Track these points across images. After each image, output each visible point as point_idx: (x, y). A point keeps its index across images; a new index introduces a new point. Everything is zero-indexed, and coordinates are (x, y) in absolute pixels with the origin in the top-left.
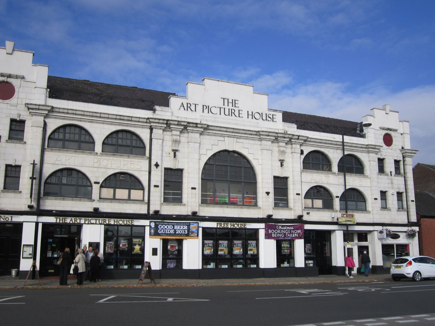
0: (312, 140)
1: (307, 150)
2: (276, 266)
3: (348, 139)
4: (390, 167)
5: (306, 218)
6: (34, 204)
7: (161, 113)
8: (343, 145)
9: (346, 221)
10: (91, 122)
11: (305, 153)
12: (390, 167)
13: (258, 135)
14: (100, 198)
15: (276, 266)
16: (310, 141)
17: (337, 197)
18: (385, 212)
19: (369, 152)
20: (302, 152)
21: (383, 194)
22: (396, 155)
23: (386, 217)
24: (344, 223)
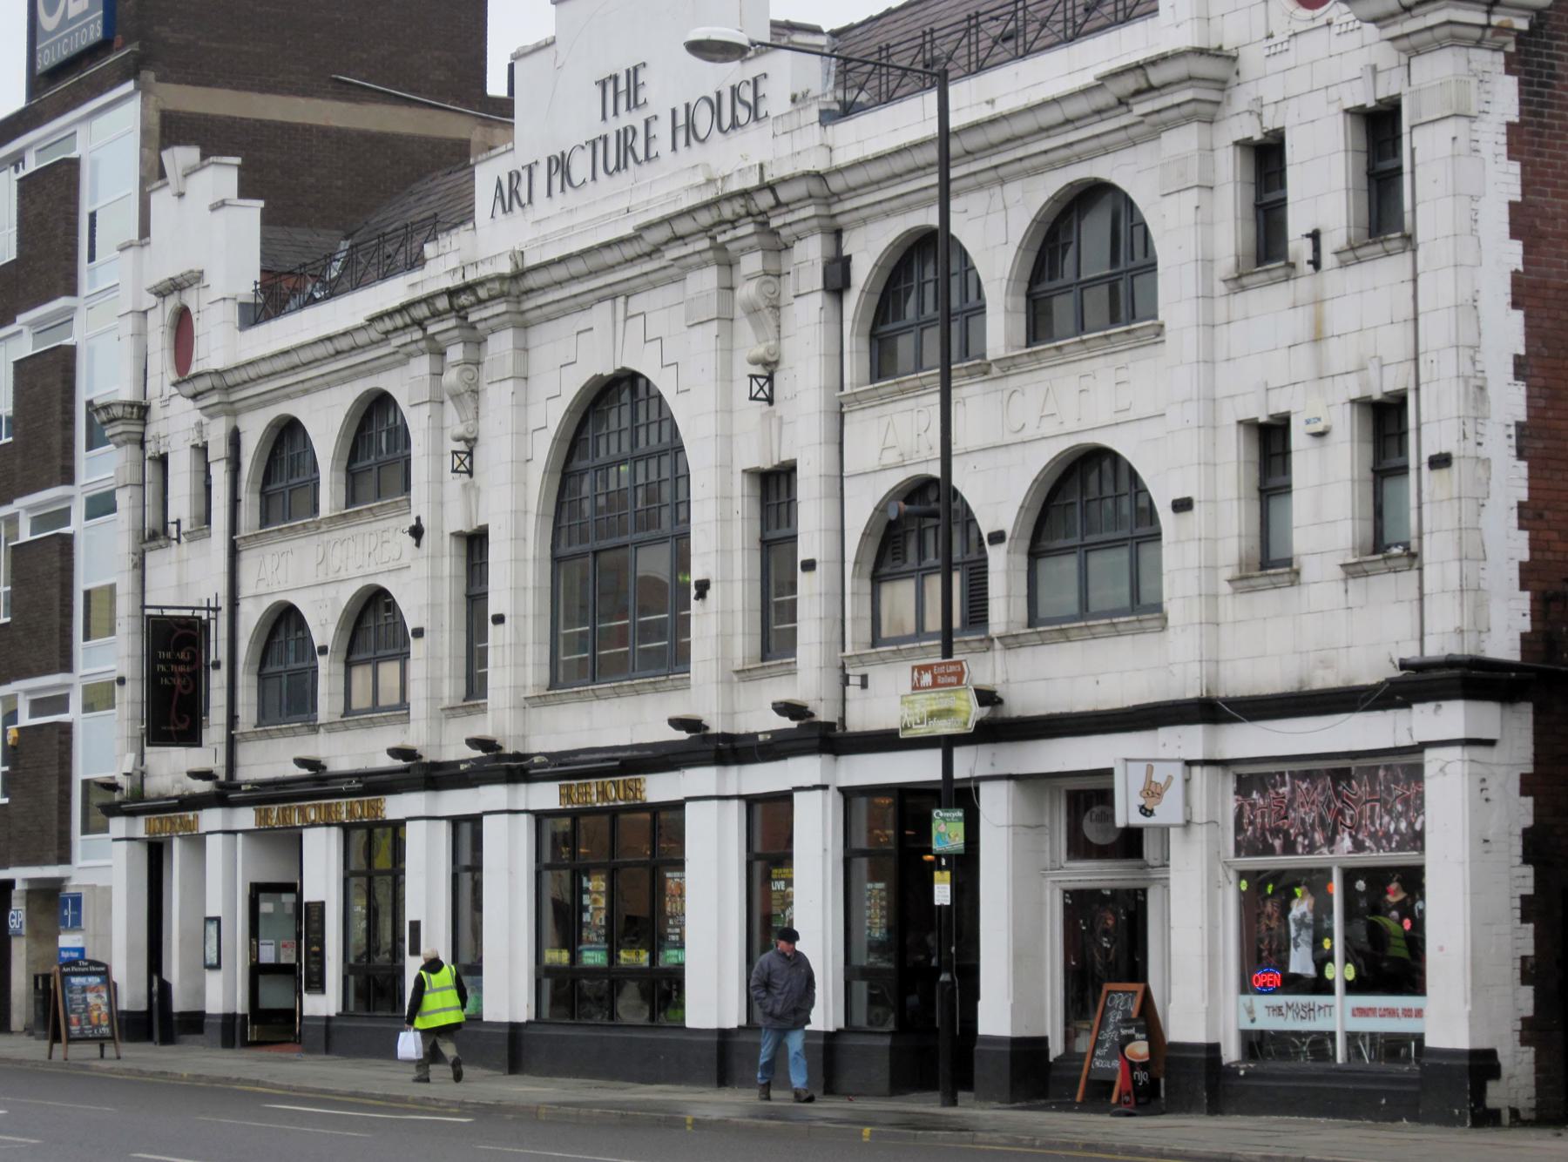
0: (855, 178)
1: (868, 251)
2: (690, 1023)
3: (971, 99)
4: (1322, 191)
5: (866, 714)
6: (218, 766)
7: (443, 264)
8: (945, 162)
9: (933, 715)
10: (306, 392)
11: (862, 271)
12: (1322, 191)
13: (647, 253)
14: (348, 710)
15: (690, 1023)
16: (853, 190)
17: (997, 537)
18: (1267, 601)
19: (1156, 127)
20: (837, 278)
21: (1271, 440)
22: (1354, 65)
23: (1269, 645)
24: (922, 731)
